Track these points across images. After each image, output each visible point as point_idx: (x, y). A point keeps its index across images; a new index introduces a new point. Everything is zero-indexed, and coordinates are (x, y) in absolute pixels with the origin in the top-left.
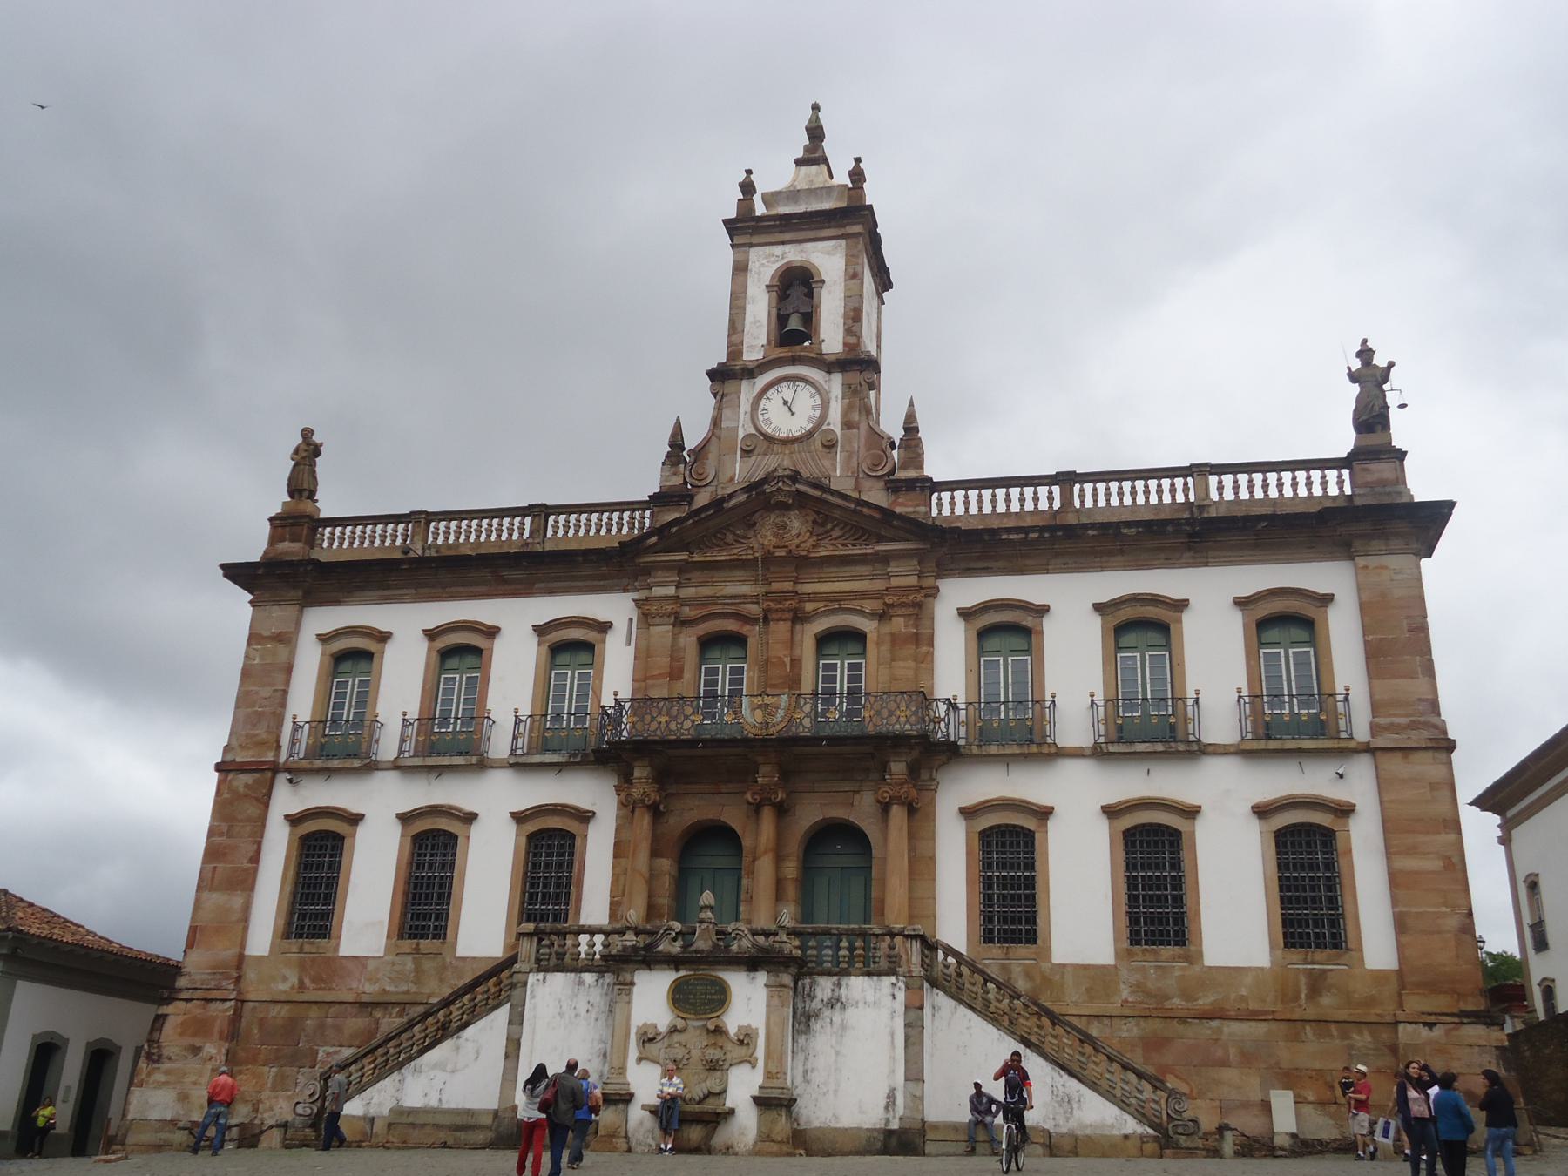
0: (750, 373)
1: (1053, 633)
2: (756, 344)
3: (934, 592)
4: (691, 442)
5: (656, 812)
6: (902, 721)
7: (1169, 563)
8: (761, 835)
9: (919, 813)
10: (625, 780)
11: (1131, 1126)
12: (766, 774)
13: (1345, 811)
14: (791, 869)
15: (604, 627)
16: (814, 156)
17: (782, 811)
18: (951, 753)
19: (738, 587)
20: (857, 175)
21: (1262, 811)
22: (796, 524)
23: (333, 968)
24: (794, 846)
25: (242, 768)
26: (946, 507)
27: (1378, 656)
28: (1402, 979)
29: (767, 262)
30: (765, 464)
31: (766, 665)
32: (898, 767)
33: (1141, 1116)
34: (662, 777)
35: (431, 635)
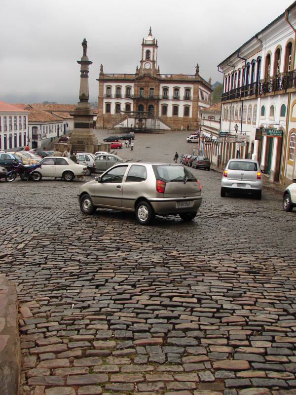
0: (144, 62)
1: (169, 89)
2: (144, 59)
3: (159, 85)
4: (138, 69)
5: (137, 104)
6: (157, 98)
7: (179, 84)
8: (145, 106)
9: (158, 105)
10: (134, 101)
11: (170, 129)
12: (146, 101)
13: (190, 106)
14: (148, 109)
15: (131, 86)
16: (150, 34)
17: (147, 104)
18: (160, 100)
19: (144, 84)
20: (154, 40)
21: (184, 105)
22: (148, 78)
23: (111, 115)
24: (148, 106)
25: (101, 98)
26: (162, 77)
27: (194, 93)
28: (192, 118)
29: (146, 49)
30: (146, 72)
31: (145, 91)
32: (156, 101)
33: (170, 127)
34: (137, 101)
35: (116, 86)
